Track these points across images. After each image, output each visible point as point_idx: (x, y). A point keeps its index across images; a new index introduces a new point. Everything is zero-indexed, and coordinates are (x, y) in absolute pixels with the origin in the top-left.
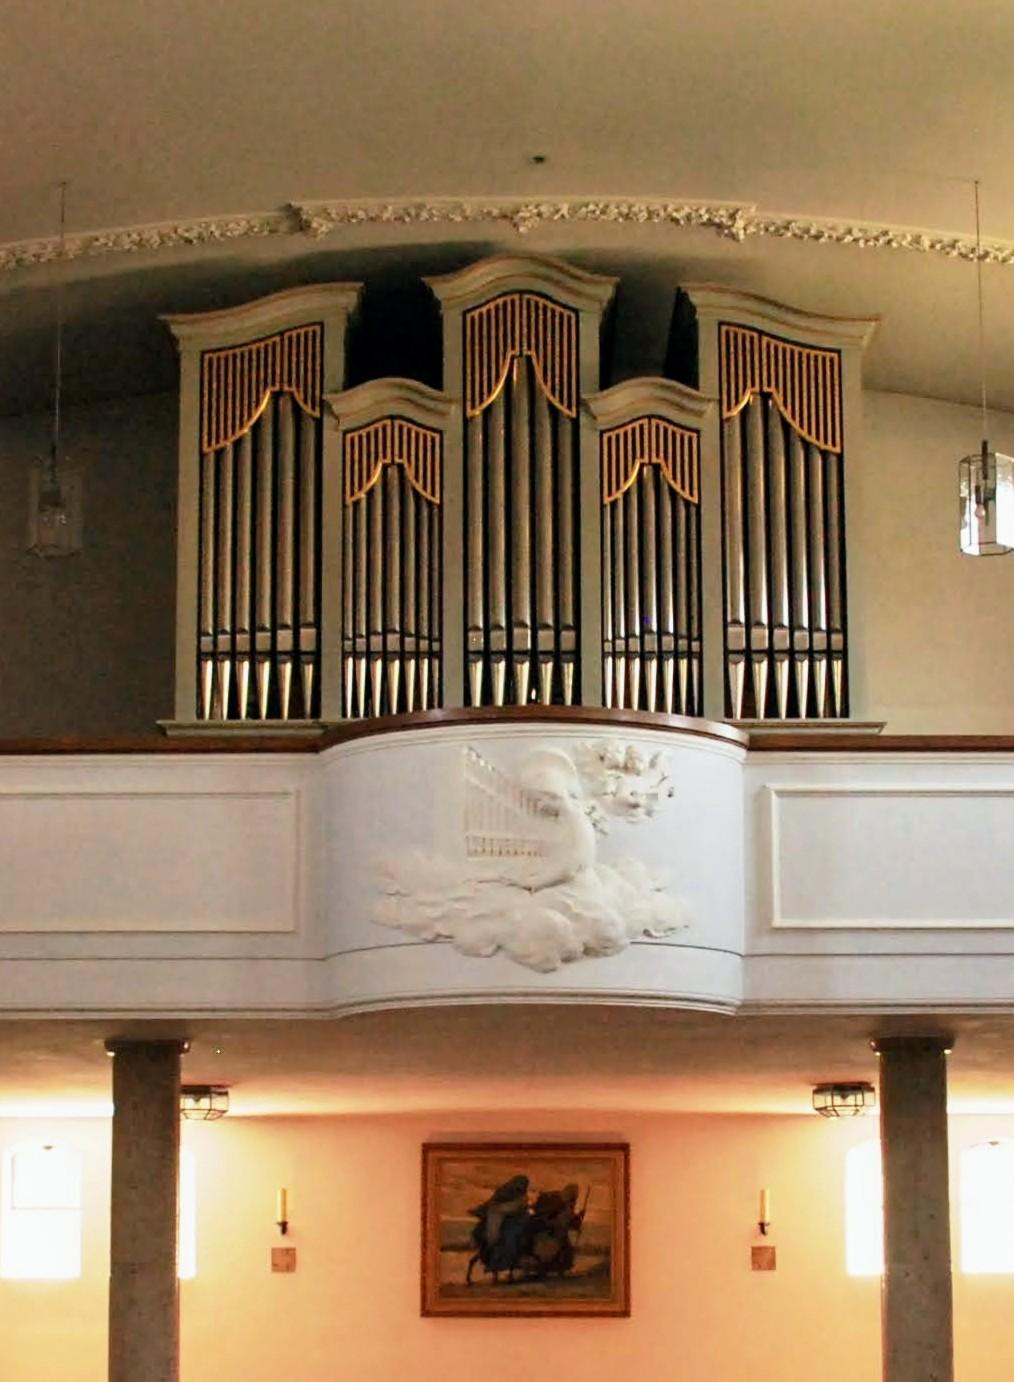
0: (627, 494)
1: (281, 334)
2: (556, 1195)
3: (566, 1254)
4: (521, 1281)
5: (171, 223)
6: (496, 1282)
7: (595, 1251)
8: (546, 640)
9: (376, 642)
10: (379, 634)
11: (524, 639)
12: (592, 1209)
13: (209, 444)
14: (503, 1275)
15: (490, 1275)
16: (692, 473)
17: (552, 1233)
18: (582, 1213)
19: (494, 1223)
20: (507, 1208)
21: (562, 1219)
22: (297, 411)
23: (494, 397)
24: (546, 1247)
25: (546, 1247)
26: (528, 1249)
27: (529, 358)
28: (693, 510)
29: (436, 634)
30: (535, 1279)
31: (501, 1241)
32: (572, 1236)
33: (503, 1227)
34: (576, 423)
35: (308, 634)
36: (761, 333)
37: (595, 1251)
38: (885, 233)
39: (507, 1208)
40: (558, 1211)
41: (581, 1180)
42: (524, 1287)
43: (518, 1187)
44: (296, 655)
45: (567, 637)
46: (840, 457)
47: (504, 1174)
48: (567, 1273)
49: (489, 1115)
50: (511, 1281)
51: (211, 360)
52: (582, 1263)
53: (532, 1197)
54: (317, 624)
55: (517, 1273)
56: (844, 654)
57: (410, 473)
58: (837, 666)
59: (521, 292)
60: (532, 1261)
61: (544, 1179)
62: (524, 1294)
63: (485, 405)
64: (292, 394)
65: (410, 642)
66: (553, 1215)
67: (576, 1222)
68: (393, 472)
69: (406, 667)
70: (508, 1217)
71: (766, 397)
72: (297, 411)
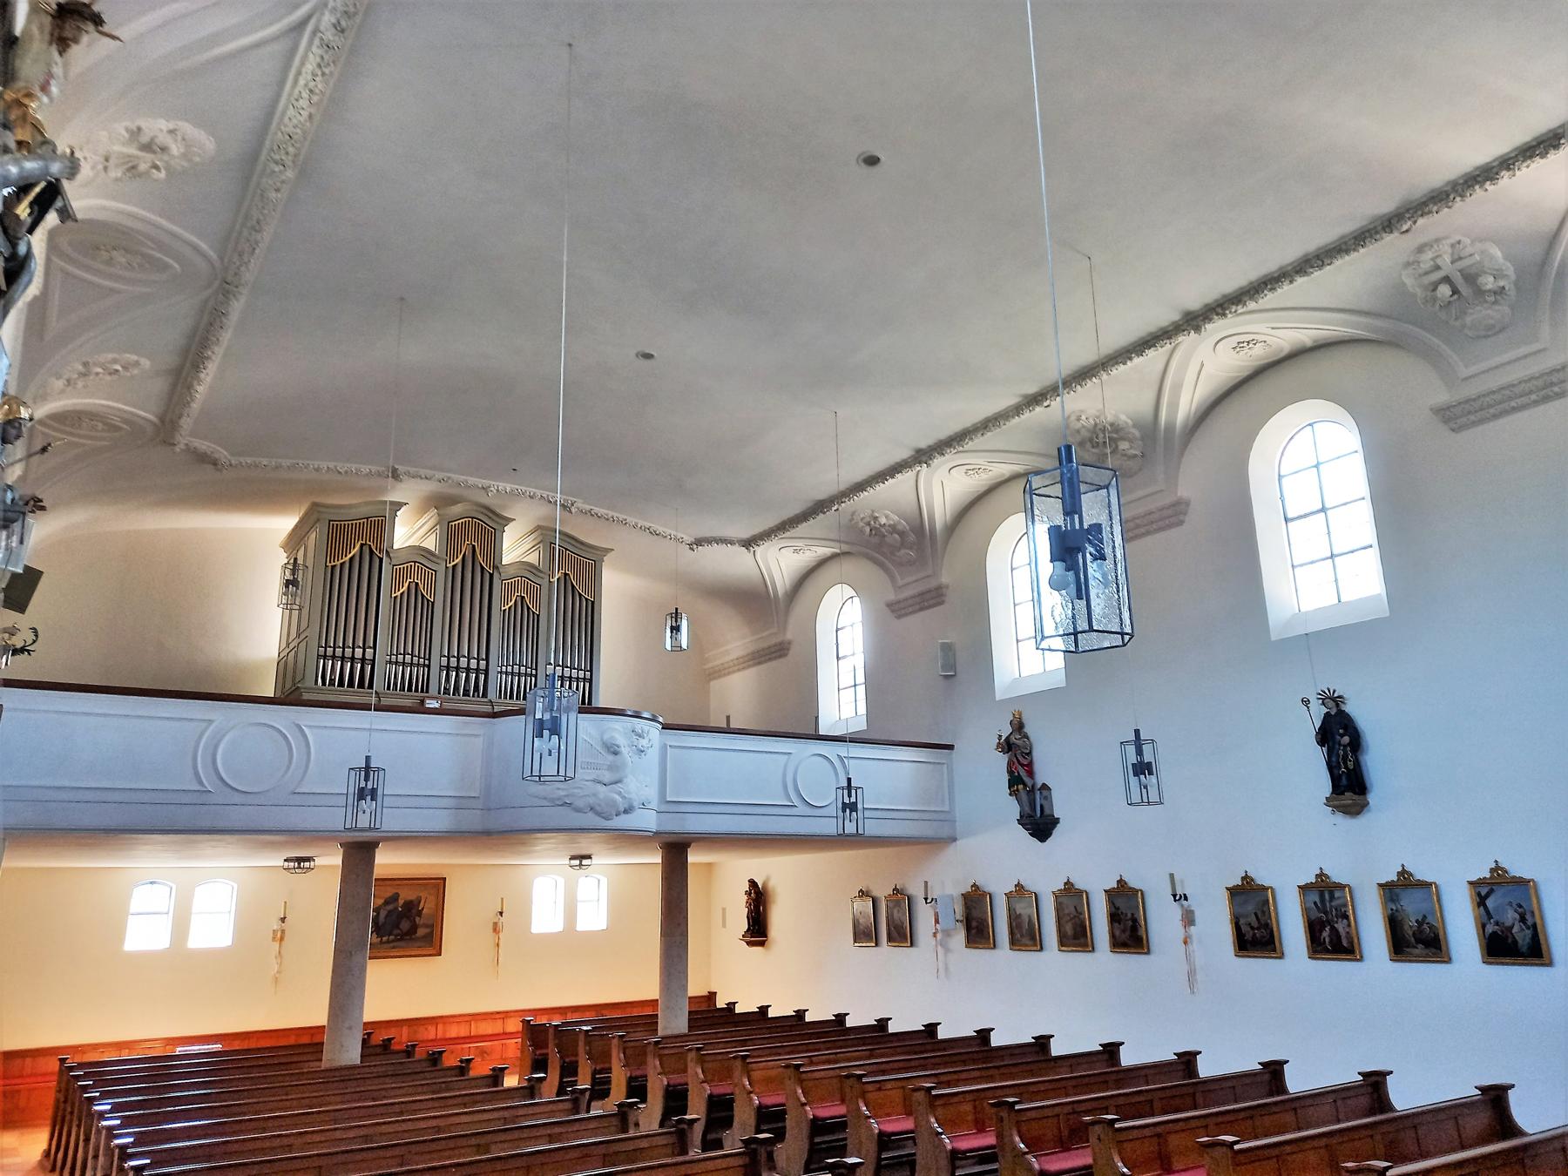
0: (510, 608)
1: (367, 518)
2: (411, 902)
3: (414, 928)
4: (393, 941)
5: (335, 464)
6: (381, 942)
7: (426, 926)
8: (473, 664)
9: (400, 658)
10: (475, 658)
11: (463, 661)
12: (427, 907)
13: (330, 562)
14: (385, 939)
15: (379, 939)
16: (537, 599)
17: (408, 918)
18: (423, 909)
19: (383, 914)
20: (390, 907)
21: (414, 911)
22: (371, 552)
23: (355, 550)
24: (405, 925)
25: (405, 925)
26: (398, 927)
27: (474, 546)
28: (536, 616)
29: (427, 657)
30: (399, 940)
31: (384, 924)
32: (417, 919)
33: (387, 917)
34: (491, 576)
35: (369, 652)
36: (566, 549)
37: (426, 926)
38: (626, 520)
39: (390, 907)
40: (411, 908)
41: (423, 895)
42: (392, 945)
43: (395, 898)
44: (363, 660)
45: (483, 663)
46: (593, 603)
47: (389, 892)
48: (413, 937)
49: (421, 865)
50: (388, 942)
51: (333, 525)
52: (421, 932)
53: (401, 902)
54: (375, 648)
55: (392, 937)
56: (591, 681)
57: (421, 586)
58: (587, 685)
59: (472, 518)
60: (399, 931)
61: (406, 895)
62: (394, 948)
63: (455, 563)
64: (370, 545)
65: (415, 659)
66: (410, 910)
67: (419, 913)
68: (413, 585)
69: (345, 667)
70: (389, 912)
71: (566, 574)
72: (371, 552)
